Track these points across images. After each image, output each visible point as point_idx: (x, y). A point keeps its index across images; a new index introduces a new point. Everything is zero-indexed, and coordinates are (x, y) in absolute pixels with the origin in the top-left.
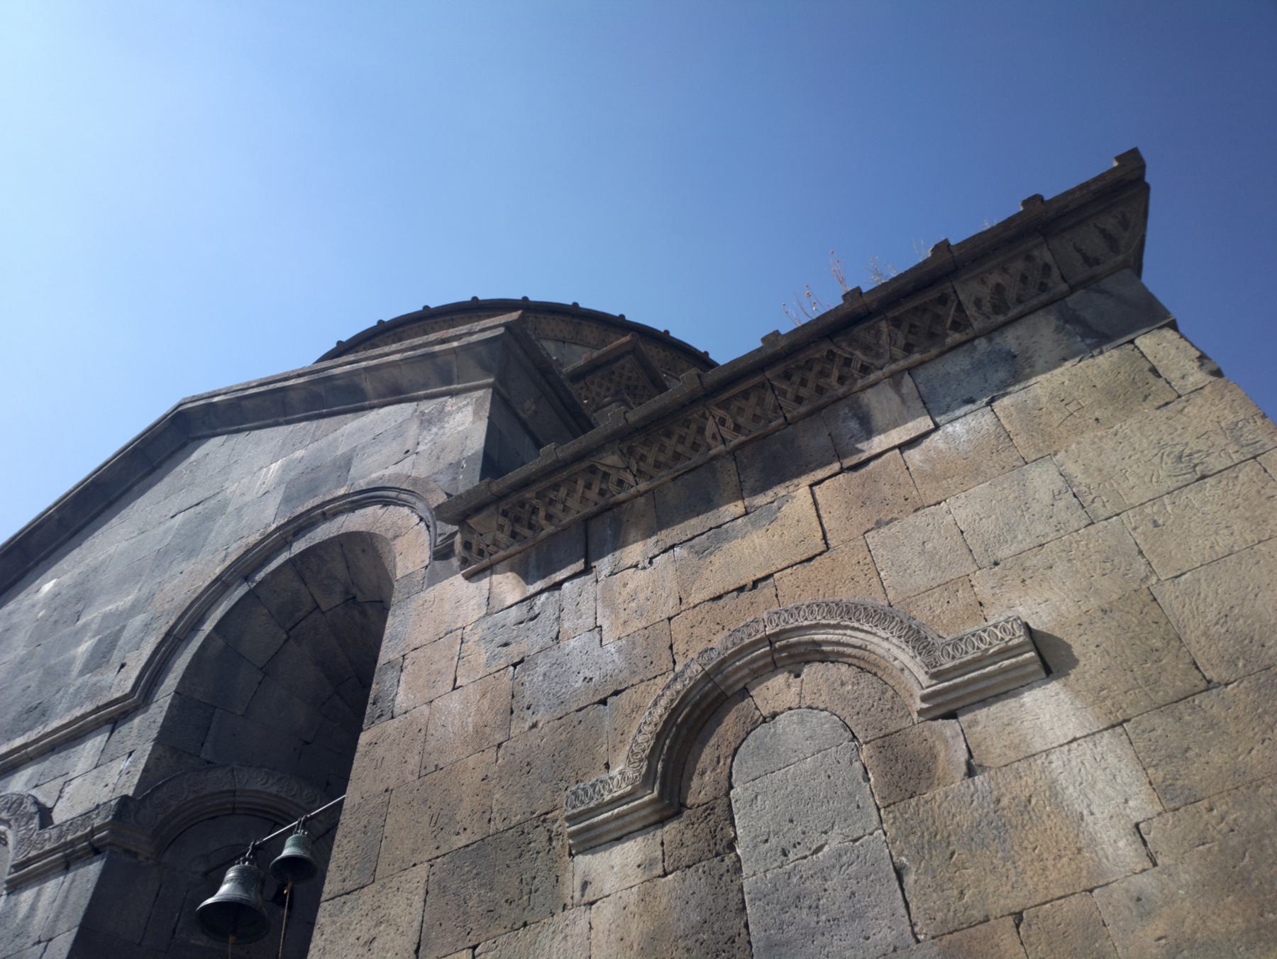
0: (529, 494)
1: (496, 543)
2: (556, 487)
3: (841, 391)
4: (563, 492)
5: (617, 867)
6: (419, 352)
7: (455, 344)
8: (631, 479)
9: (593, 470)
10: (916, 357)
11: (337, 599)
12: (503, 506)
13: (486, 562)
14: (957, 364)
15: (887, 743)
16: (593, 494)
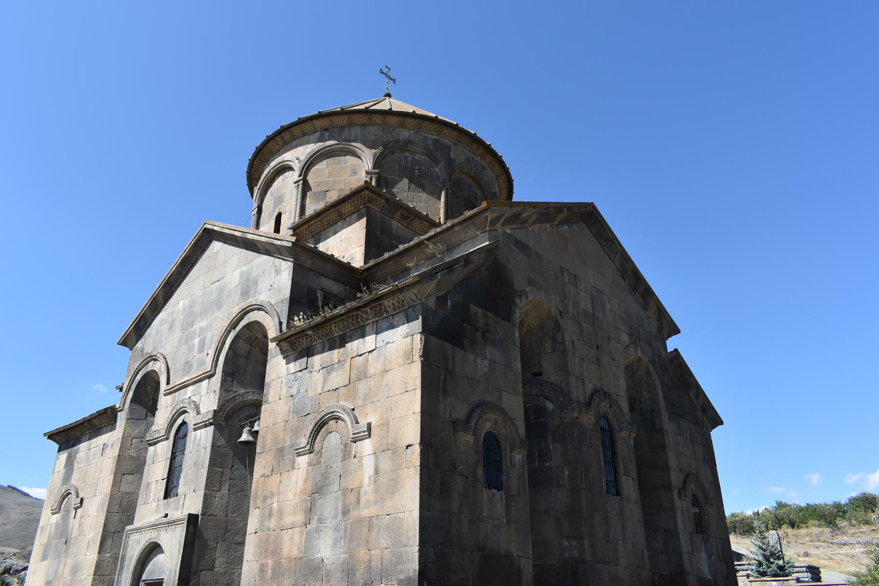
7: (279, 243)
14: (384, 324)
15: (346, 445)
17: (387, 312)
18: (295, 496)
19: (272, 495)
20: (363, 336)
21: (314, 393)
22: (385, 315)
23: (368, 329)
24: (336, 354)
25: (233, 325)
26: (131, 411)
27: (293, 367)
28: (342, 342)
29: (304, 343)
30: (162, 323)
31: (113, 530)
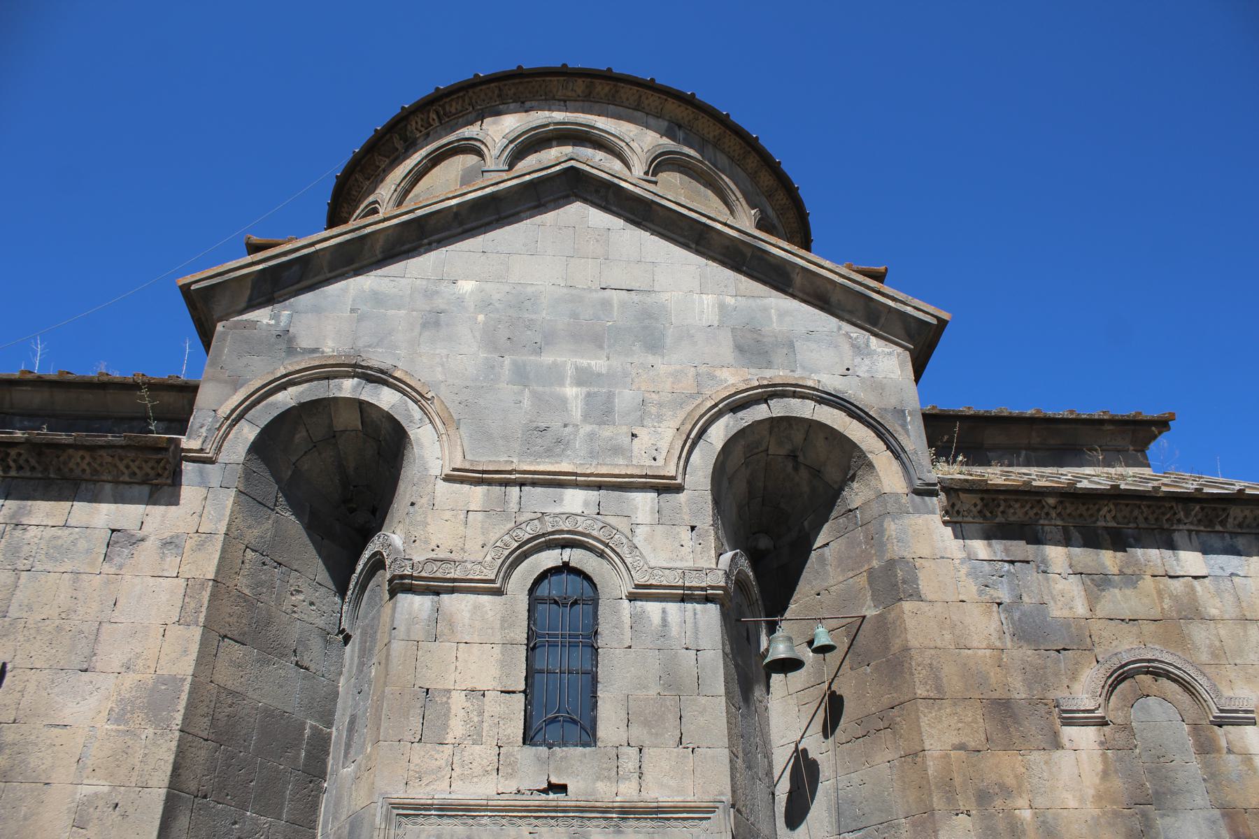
0: (1001, 497)
1: (969, 511)
2: (1017, 501)
3: (1166, 526)
4: (1017, 506)
5: (1085, 737)
6: (858, 288)
8: (1054, 515)
9: (1039, 501)
10: (1202, 528)
11: (783, 452)
12: (985, 496)
13: (960, 519)
14: (1215, 541)
15: (1195, 727)
16: (1031, 513)
17: (1223, 523)
18: (1082, 800)
19: (1006, 792)
20: (1172, 546)
21: (1066, 613)
22: (1218, 528)
23: (1177, 537)
24: (1109, 560)
25: (736, 405)
26: (248, 474)
27: (980, 548)
28: (1119, 542)
29: (1017, 514)
30: (378, 299)
31: (193, 786)
